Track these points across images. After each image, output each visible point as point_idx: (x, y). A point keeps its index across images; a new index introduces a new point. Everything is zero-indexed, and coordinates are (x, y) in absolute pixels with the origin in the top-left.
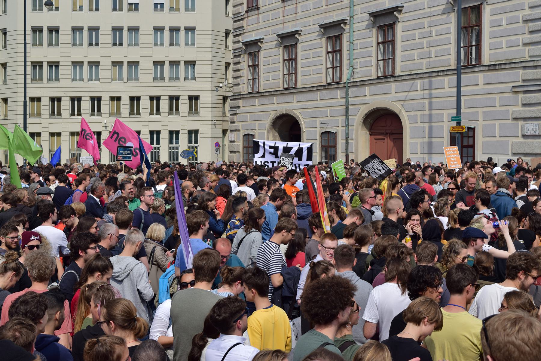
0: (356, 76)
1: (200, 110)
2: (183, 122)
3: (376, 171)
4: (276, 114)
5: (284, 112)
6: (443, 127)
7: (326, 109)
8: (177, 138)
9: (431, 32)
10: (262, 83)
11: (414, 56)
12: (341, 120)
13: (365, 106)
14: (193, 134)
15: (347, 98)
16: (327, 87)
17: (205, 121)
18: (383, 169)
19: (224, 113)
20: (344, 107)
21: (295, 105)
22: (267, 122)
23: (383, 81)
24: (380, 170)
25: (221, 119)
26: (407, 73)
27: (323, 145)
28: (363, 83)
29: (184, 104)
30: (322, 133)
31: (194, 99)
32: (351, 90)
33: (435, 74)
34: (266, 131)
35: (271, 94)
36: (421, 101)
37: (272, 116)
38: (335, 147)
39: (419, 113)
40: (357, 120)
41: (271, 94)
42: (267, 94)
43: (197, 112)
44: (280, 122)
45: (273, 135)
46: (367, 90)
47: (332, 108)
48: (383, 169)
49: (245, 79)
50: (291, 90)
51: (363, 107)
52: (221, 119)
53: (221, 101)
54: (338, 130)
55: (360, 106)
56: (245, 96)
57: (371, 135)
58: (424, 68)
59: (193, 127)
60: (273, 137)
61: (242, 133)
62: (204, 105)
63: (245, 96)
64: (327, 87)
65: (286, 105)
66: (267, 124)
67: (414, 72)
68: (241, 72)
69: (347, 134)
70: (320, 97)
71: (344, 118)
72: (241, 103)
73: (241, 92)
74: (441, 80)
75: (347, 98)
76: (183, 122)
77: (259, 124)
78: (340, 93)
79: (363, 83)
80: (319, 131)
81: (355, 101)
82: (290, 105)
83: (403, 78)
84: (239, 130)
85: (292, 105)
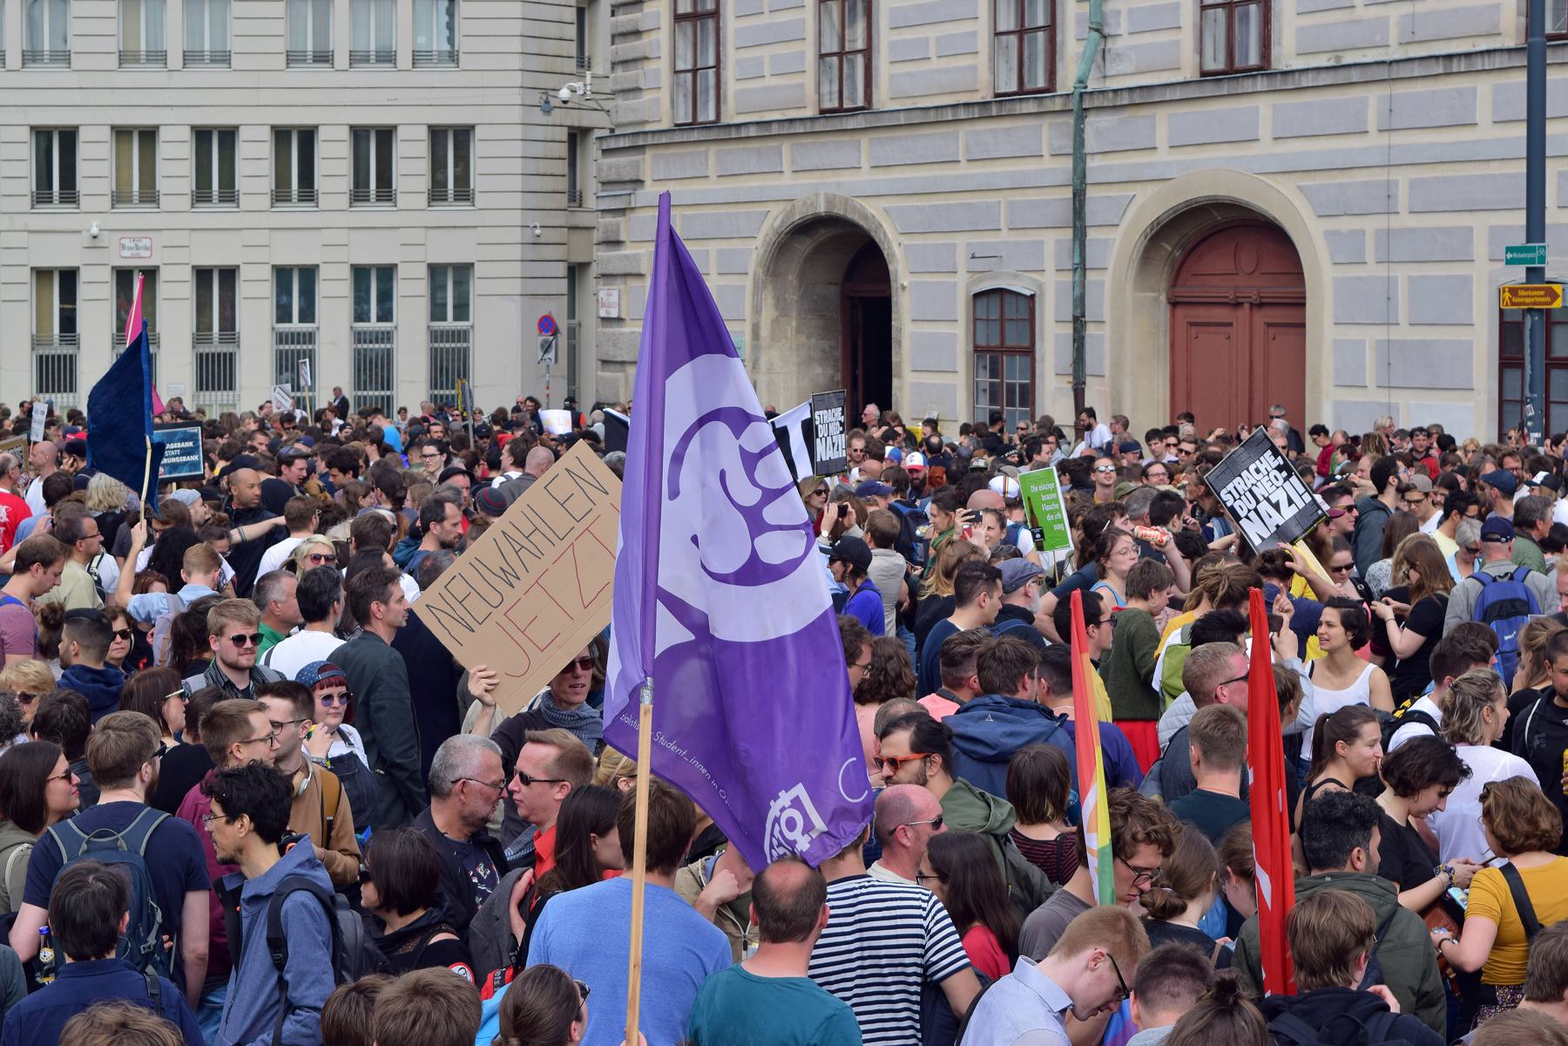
0: (1112, 68)
1: (476, 182)
2: (409, 233)
3: (1264, 507)
5: (822, 209)
6: (1466, 281)
7: (991, 198)
8: (386, 297)
10: (731, 87)
12: (1054, 243)
13: (1151, 189)
14: (450, 283)
16: (998, 106)
17: (493, 233)
18: (1290, 502)
19: (575, 197)
20: (1068, 193)
21: (865, 178)
22: (752, 244)
23: (1225, 88)
24: (1276, 506)
25: (560, 219)
26: (1323, 61)
27: (982, 342)
28: (1144, 97)
29: (411, 162)
30: (977, 296)
31: (451, 145)
33: (1439, 68)
34: (748, 282)
35: (768, 131)
36: (1380, 176)
37: (774, 220)
38: (1029, 352)
39: (1371, 225)
40: (1117, 240)
41: (768, 131)
42: (753, 132)
43: (464, 192)
44: (805, 246)
46: (1162, 123)
47: (1018, 196)
48: (1290, 502)
49: (662, 67)
50: (845, 114)
51: (1144, 194)
52: (560, 219)
53: (562, 150)
54: (1040, 286)
55: (1129, 191)
56: (664, 139)
57: (1174, 304)
58: (1393, 38)
59: (449, 251)
60: (777, 306)
62: (498, 163)
63: (664, 139)
64: (998, 106)
65: (830, 178)
66: (754, 250)
67: (1349, 58)
68: (645, 39)
69: (1080, 302)
70: (968, 150)
71: (1068, 234)
72: (648, 165)
73: (644, 122)
74: (1460, 92)
76: (409, 233)
77: (720, 252)
78: (1050, 134)
79: (1144, 97)
80: (962, 286)
82: (846, 177)
83: (1306, 81)
85: (855, 180)
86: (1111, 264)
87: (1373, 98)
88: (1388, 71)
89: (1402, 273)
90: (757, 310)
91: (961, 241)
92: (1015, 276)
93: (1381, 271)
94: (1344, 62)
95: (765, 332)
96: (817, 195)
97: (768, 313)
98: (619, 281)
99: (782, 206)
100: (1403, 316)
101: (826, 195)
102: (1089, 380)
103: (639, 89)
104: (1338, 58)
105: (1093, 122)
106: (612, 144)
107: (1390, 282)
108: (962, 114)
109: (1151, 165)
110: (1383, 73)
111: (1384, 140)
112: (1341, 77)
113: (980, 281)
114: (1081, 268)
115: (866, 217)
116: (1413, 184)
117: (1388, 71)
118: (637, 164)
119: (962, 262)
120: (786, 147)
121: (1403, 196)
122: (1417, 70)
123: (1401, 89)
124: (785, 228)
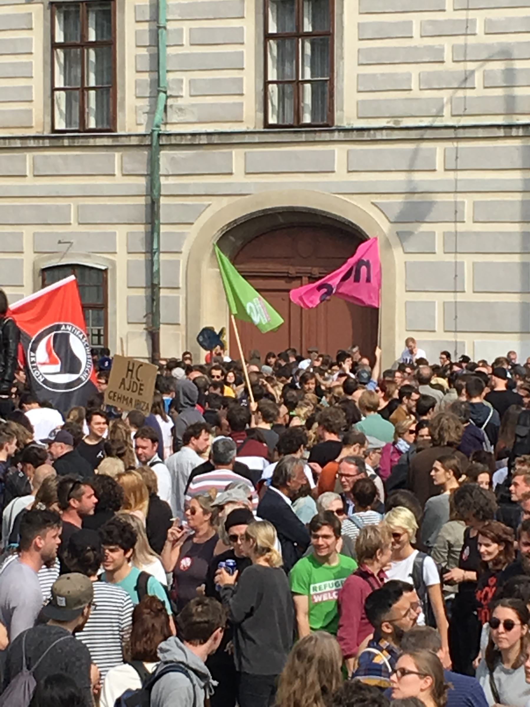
0: (173, 117)
9: (468, 23)
11: (409, 80)
15: (152, 175)
16: (55, 139)
30: (44, 270)
32: (164, 155)
33: (501, 132)
38: (104, 307)
46: (237, 156)
51: (217, 205)
54: (113, 263)
55: (206, 201)
64: (55, 139)
70: (34, 166)
71: (141, 229)
75: (152, 175)
81: (186, 185)
83: (379, 135)
86: (185, 249)
87: (439, 149)
88: (455, 133)
89: (467, 261)
92: (87, 256)
93: (450, 258)
94: (403, 125)
100: (468, 286)
102: (163, 328)
104: (396, 122)
105: (165, 156)
107: (457, 267)
108: (31, 143)
109: (230, 184)
110: (451, 133)
111: (451, 175)
112: (396, 135)
113: (50, 259)
114: (151, 252)
116: (475, 204)
117: (455, 133)
119: (27, 246)
121: (468, 212)
122: (481, 133)
123: (462, 145)
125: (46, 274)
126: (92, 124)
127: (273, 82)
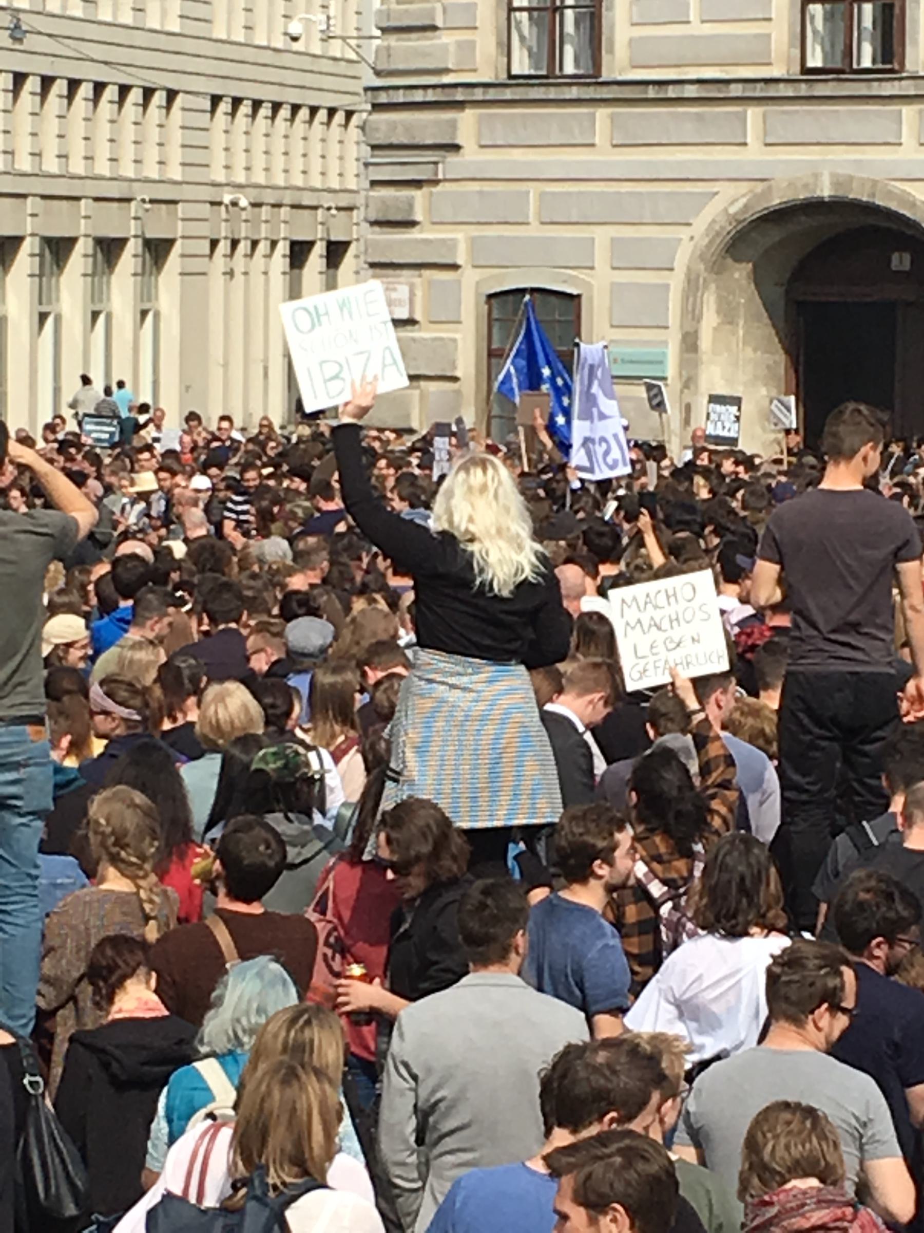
4: (757, 197)
5: (826, 191)
21: (909, 153)
22: (683, 233)
34: (676, 282)
37: (729, 203)
42: (691, 91)
44: (775, 234)
45: (720, 300)
56: (492, 94)
61: (471, 288)
63: (492, 94)
72: (466, 124)
73: (446, 71)
84: (455, 267)
90: (692, 314)
91: (602, 235)
95: (705, 342)
96: (816, 176)
97: (710, 319)
98: (406, 273)
99: (744, 187)
101: (832, 175)
103: (434, 28)
106: (383, 98)
115: (913, 205)
118: (453, 125)
120: (753, 113)
124: (749, 216)
125: (493, 301)
126: (569, 68)
127: (521, 9)
